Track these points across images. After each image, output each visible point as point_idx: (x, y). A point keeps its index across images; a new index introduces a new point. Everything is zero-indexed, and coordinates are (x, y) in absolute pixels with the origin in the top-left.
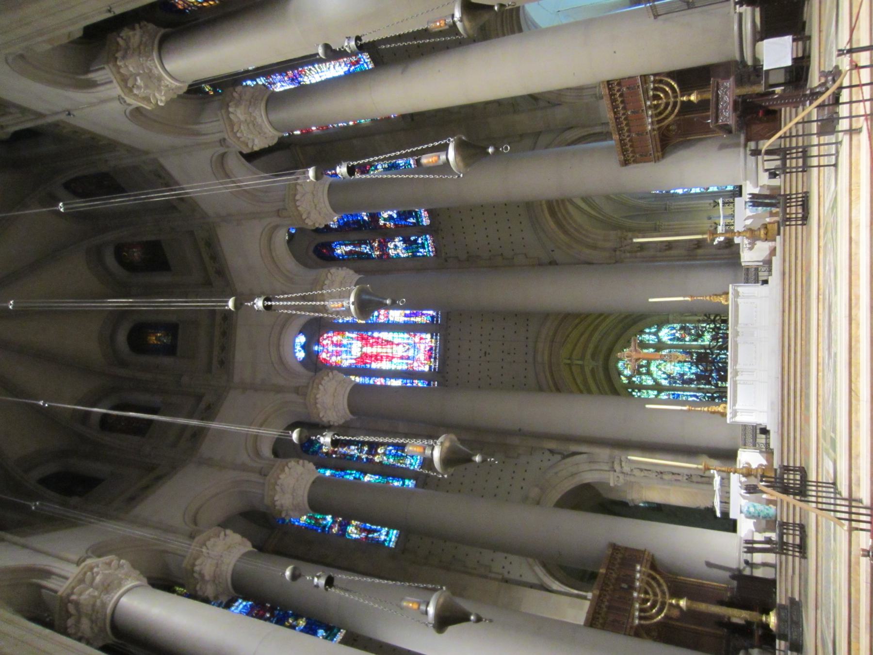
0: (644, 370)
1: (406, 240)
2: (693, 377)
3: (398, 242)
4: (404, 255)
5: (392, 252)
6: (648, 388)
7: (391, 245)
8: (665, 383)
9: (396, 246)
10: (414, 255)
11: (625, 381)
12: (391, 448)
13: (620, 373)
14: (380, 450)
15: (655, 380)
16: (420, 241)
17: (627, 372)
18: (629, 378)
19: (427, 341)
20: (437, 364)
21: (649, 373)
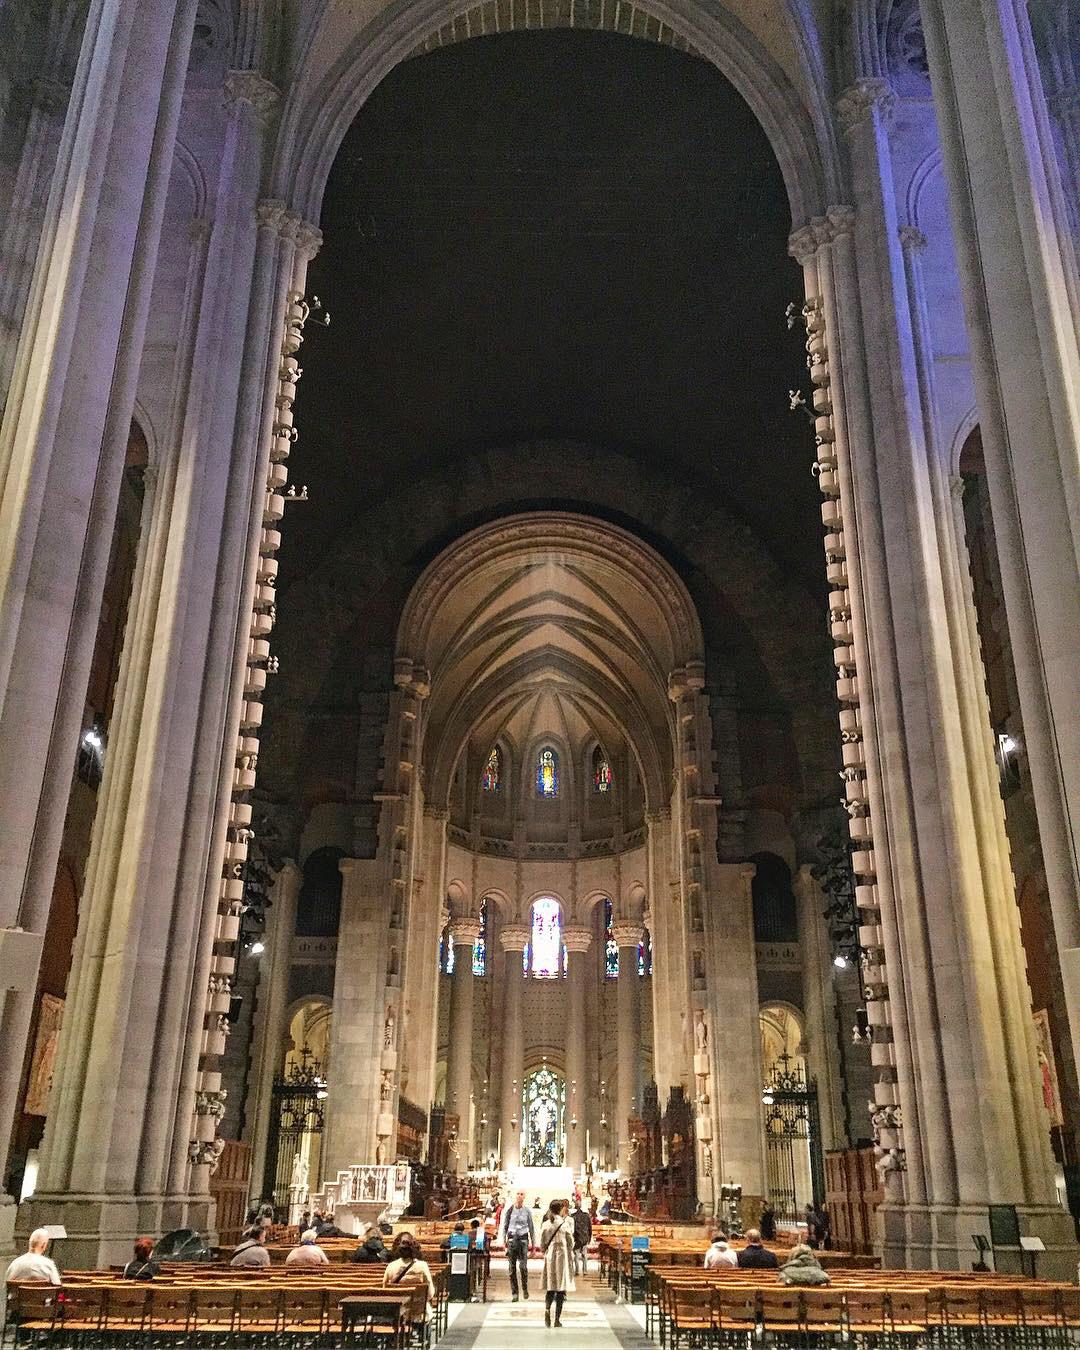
0: (541, 1091)
1: (616, 954)
2: (537, 1130)
3: (615, 950)
4: (609, 951)
5: (610, 943)
6: (528, 1093)
7: (614, 943)
8: (531, 1108)
9: (613, 947)
10: (607, 960)
11: (533, 1076)
12: (483, 947)
13: (538, 1072)
14: (482, 941)
15: (533, 1100)
16: (616, 966)
17: (539, 1079)
18: (534, 1080)
19: (553, 969)
20: (537, 977)
21: (539, 1095)
